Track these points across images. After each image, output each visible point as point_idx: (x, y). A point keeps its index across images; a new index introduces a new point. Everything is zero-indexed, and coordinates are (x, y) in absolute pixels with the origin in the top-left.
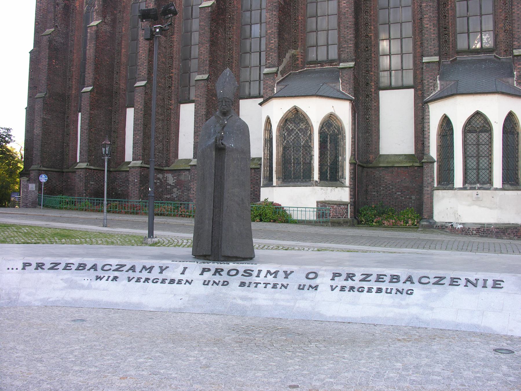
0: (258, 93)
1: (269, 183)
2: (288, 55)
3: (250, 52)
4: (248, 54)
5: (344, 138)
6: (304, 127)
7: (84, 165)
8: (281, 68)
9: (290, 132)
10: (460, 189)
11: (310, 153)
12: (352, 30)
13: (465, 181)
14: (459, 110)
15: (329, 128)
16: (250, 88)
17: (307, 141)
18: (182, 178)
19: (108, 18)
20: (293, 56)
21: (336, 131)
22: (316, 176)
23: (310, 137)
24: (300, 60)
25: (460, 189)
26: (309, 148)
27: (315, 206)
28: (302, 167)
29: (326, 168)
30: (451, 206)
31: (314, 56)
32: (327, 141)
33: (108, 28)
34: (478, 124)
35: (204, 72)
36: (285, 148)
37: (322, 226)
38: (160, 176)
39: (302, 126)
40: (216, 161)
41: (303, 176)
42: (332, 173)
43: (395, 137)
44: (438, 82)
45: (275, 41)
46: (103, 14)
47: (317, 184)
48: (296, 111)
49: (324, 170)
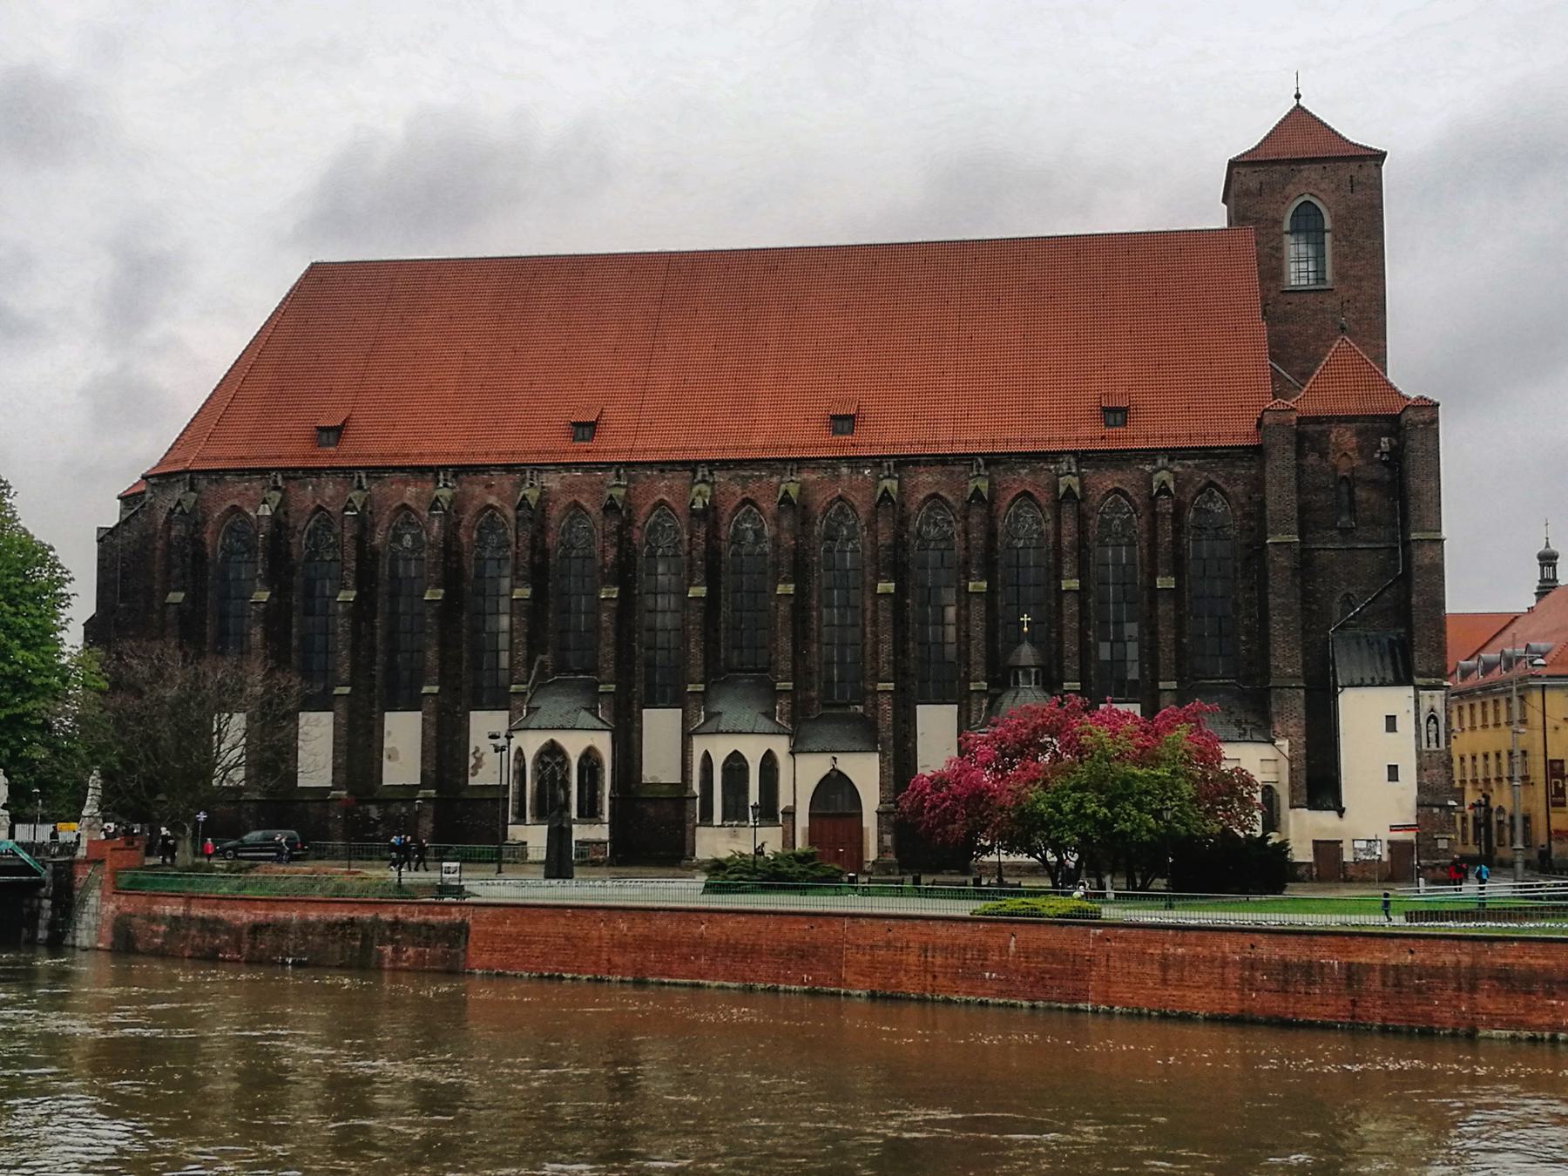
1: (520, 818)
9: (546, 765)
14: (720, 748)
18: (392, 810)
20: (542, 662)
23: (568, 771)
26: (565, 784)
30: (713, 843)
34: (736, 764)
48: (552, 741)
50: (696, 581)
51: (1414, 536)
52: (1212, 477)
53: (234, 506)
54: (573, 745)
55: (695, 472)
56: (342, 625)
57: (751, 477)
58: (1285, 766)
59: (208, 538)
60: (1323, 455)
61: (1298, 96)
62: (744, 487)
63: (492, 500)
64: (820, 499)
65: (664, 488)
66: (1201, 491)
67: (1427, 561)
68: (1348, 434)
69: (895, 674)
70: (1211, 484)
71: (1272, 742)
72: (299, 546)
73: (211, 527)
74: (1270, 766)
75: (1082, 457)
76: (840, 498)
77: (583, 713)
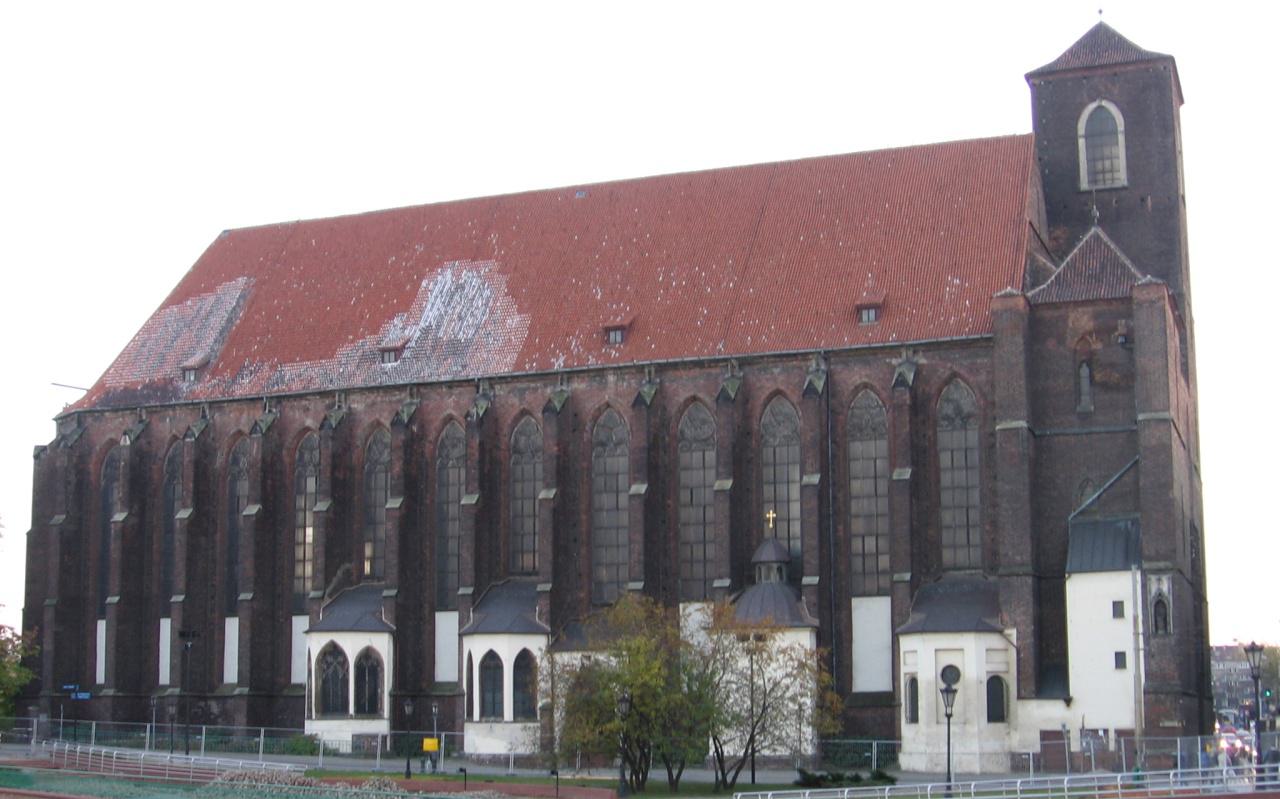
2: (339, 573)
5: (383, 670)
7: (111, 692)
8: (328, 591)
9: (329, 665)
10: (477, 722)
13: (483, 714)
19: (136, 507)
20: (348, 570)
22: (352, 710)
23: (347, 670)
24: (355, 575)
25: (477, 722)
27: (350, 739)
34: (492, 661)
36: (325, 682)
38: (202, 704)
39: (341, 659)
46: (128, 504)
47: (351, 718)
51: (1141, 417)
52: (956, 368)
53: (111, 440)
54: (352, 645)
55: (478, 387)
56: (180, 540)
57: (528, 388)
58: (1013, 653)
59: (92, 467)
60: (1061, 340)
61: (1100, 12)
62: (522, 399)
63: (309, 422)
64: (590, 406)
65: (451, 404)
66: (947, 382)
67: (1154, 442)
68: (1086, 318)
69: (645, 573)
70: (955, 375)
71: (1001, 632)
73: (94, 458)
74: (999, 657)
75: (827, 356)
76: (608, 405)
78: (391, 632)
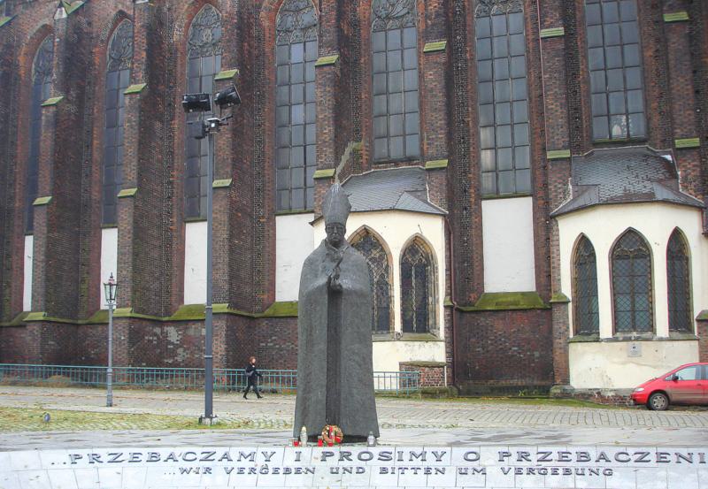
0: (302, 205)
2: (348, 151)
3: (289, 146)
4: (288, 149)
5: (435, 270)
6: (378, 255)
10: (608, 340)
11: (387, 294)
12: (442, 113)
13: (616, 327)
14: (603, 229)
15: (413, 255)
16: (290, 199)
17: (382, 276)
18: (191, 332)
19: (73, 93)
21: (424, 260)
23: (387, 269)
24: (365, 157)
25: (608, 340)
27: (397, 369)
28: (376, 313)
29: (411, 314)
30: (596, 365)
31: (385, 151)
32: (411, 275)
33: (73, 108)
34: (631, 248)
35: (225, 176)
37: (409, 397)
38: (157, 330)
39: (375, 253)
40: (329, 307)
41: (378, 326)
42: (420, 321)
43: (507, 267)
44: (570, 187)
45: (330, 131)
46: (64, 87)
47: (398, 338)
49: (408, 318)
50: (549, 21)
53: (45, 26)
54: (395, 232)
56: (128, 119)
59: (21, 60)
72: (100, 57)
73: (24, 49)
77: (406, 195)
78: (444, 216)
